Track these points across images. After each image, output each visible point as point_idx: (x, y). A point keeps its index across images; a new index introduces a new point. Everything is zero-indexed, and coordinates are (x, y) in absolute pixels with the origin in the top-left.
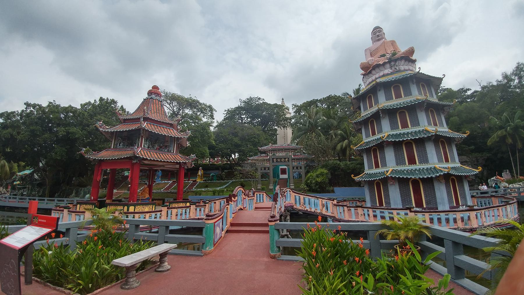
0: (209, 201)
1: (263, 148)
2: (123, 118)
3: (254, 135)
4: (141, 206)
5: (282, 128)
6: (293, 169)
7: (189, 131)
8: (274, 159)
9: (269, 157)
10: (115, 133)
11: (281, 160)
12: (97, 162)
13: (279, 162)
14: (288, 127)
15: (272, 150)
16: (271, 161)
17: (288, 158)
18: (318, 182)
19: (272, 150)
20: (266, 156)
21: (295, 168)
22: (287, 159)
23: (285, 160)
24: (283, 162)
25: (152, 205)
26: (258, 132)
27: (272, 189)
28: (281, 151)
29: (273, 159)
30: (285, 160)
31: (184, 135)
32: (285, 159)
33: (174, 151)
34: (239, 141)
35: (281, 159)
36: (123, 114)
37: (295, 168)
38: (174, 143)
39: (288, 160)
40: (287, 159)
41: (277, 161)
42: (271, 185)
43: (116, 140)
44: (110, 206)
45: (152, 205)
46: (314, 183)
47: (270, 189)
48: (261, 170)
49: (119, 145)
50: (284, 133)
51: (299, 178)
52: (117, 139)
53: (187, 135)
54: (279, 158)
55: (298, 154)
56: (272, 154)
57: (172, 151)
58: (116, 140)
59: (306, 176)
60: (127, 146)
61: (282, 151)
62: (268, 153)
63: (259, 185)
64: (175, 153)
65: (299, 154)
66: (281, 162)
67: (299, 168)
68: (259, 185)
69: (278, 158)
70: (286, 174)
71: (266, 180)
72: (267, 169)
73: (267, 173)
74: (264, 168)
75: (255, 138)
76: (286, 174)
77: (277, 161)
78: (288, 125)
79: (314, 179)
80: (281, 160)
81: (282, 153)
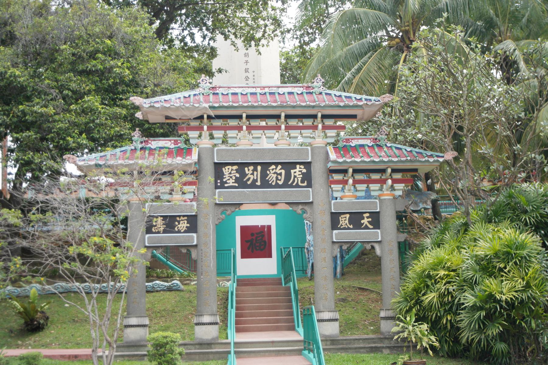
1: (160, 101)
3: (110, 37)
5: (239, 42)
6: (335, 223)
8: (226, 170)
9: (195, 157)
11: (264, 175)
13: (253, 185)
14: (263, 41)
15: (218, 117)
16: (209, 178)
17: (308, 165)
18: (499, 301)
19: (218, 117)
20: (180, 152)
21: (344, 221)
22: (297, 172)
23: (288, 176)
24: (277, 186)
26: (129, 30)
27: (209, 344)
28: (263, 123)
29: (219, 167)
30: (288, 176)
32: (289, 166)
34: (15, 65)
35: (266, 166)
37: (344, 221)
39: (307, 178)
40: (297, 172)
41: (241, 183)
42: (206, 319)
46: (474, 308)
47: (201, 344)
48: (149, 230)
50: (247, 71)
51: (343, 274)
54: (255, 165)
55: (361, 142)
56: (212, 137)
59: (403, 268)
61: (272, 122)
62: (193, 134)
63: (133, 321)
65: (369, 142)
66: (265, 184)
67: (365, 221)
68: (133, 321)
69: (248, 164)
70: (270, 256)
71: (170, 289)
72: (183, 225)
73: (184, 251)
74: (165, 217)
75: (113, 54)
76: (270, 256)
77: (241, 183)
78: (265, 32)
79: (472, 284)
80: (264, 175)
81: (269, 133)
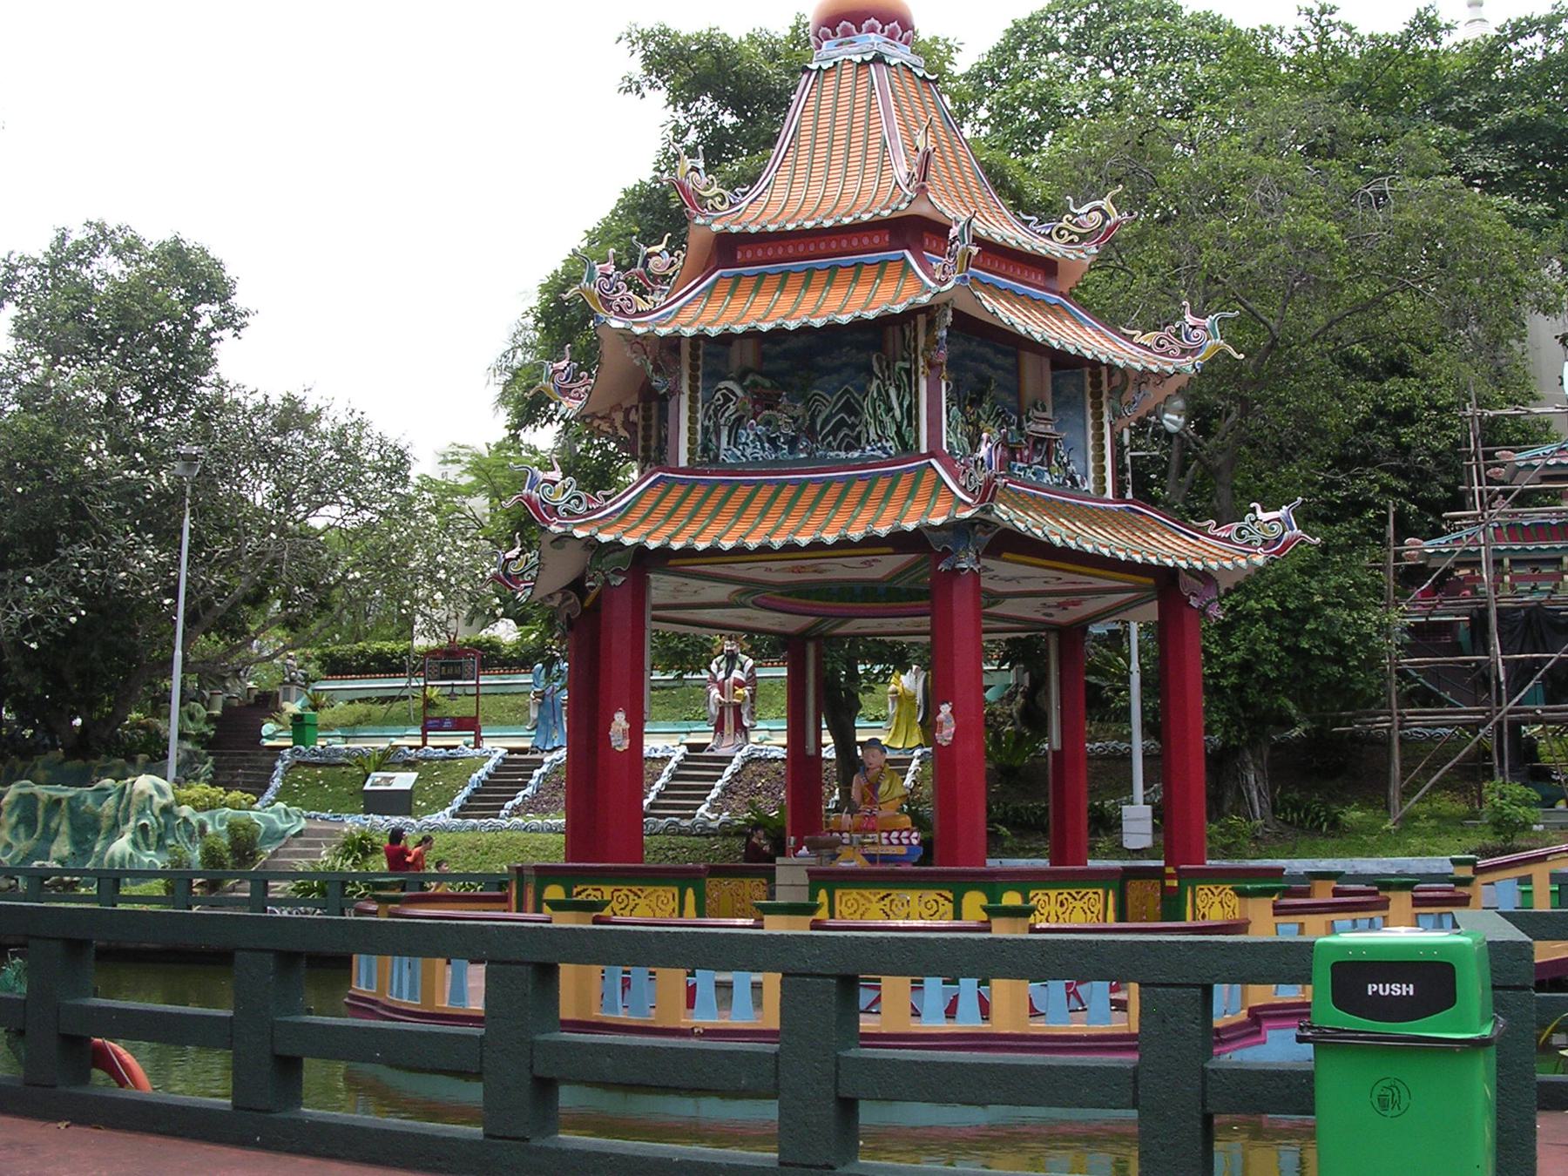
0: (1478, 871)
2: (716, 227)
4: (1053, 893)
7: (1207, 322)
10: (686, 350)
12: (618, 572)
25: (1100, 891)
31: (1166, 354)
33: (1101, 481)
36: (712, 198)
38: (1098, 416)
43: (700, 405)
44: (838, 893)
45: (1100, 891)
49: (734, 440)
52: (710, 390)
53: (1194, 352)
57: (1089, 486)
58: (700, 405)
60: (793, 443)
64: (1109, 495)
